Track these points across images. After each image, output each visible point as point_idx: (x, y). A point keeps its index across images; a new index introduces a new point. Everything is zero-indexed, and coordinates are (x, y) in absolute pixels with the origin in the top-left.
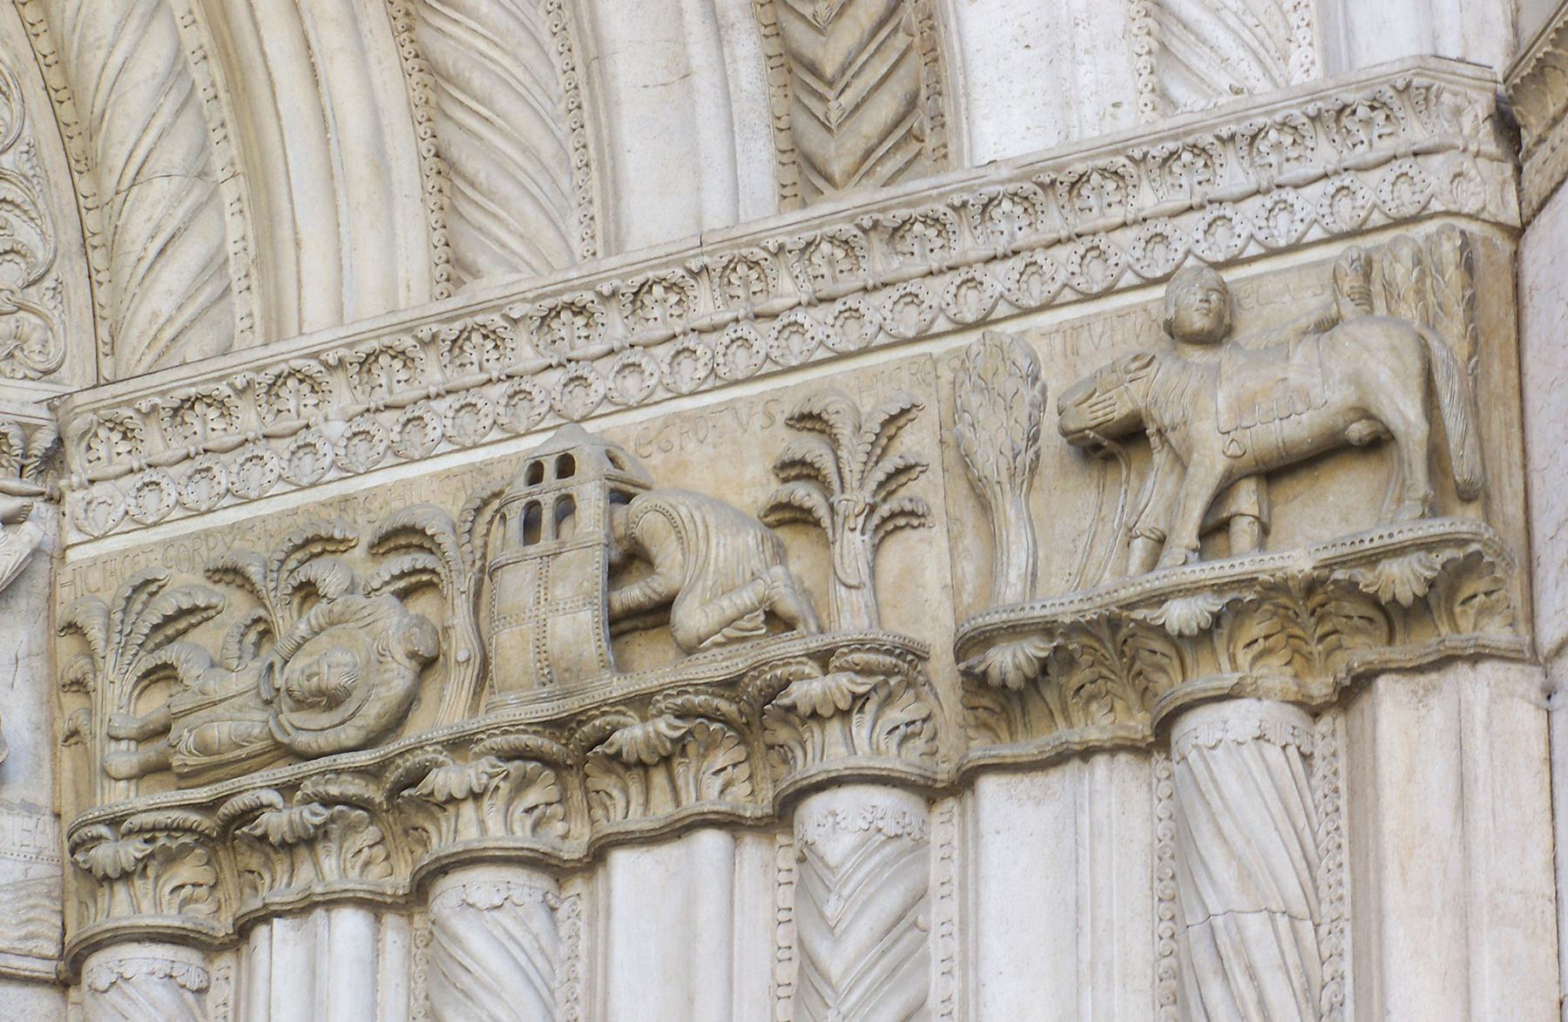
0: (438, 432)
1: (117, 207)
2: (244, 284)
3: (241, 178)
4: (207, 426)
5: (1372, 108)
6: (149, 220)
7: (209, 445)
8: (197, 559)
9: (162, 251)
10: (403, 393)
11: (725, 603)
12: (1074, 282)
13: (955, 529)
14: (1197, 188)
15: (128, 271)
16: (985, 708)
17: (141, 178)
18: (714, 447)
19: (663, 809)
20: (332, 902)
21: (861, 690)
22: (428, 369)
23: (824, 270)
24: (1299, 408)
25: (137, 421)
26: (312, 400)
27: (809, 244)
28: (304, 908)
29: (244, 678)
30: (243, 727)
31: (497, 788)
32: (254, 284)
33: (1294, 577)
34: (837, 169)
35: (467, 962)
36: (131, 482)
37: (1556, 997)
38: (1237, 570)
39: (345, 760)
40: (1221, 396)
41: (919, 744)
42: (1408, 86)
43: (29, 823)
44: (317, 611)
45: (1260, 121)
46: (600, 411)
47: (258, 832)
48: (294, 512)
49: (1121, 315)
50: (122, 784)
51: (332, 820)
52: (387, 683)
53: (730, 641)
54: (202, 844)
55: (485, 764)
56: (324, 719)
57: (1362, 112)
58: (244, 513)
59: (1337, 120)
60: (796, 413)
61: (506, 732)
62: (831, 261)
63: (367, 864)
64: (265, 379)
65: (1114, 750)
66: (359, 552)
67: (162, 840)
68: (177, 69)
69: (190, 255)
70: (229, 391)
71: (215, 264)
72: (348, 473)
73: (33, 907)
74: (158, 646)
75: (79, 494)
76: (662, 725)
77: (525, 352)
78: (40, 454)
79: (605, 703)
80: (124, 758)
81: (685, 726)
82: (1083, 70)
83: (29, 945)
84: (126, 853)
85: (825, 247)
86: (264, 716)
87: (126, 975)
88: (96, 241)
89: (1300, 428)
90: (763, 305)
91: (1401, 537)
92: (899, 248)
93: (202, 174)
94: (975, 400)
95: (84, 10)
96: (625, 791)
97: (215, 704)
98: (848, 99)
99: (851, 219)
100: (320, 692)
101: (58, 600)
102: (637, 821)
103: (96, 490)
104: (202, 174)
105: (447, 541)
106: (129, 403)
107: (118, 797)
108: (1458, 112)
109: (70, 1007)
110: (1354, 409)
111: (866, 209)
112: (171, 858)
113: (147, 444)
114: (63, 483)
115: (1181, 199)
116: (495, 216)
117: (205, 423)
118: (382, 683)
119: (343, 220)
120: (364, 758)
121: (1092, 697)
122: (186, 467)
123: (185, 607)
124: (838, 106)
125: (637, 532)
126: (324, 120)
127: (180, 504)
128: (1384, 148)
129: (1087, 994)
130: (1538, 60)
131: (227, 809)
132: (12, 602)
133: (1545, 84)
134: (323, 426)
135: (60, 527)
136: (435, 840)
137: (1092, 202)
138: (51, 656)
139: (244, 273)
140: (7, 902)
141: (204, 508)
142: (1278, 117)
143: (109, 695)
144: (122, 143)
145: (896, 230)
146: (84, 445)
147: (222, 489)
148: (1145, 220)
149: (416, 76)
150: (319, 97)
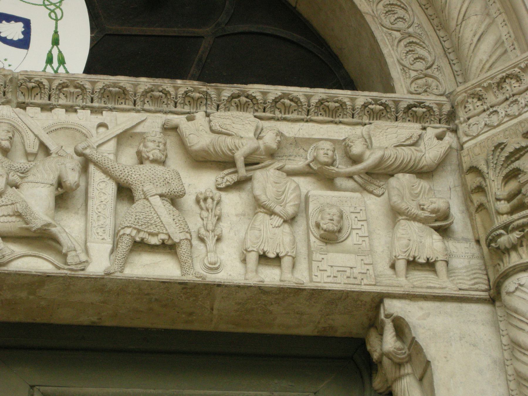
1: (457, 31)
2: (512, 47)
3: (503, 14)
4: (512, 86)
6: (472, 30)
7: (515, 92)
8: (518, 132)
9: (479, 40)
15: (467, 50)
17: (466, 18)
25: (483, 92)
32: (516, 46)
36: (484, 115)
43: (467, 245)
50: (505, 216)
69: (489, 41)
70: (519, 70)
71: (499, 42)
73: (475, 274)
74: (508, 165)
75: (464, 125)
78: (446, 113)
80: (504, 206)
83: (477, 286)
84: (513, 237)
87: (522, 283)
88: (450, 51)
93: (488, 14)
101: (463, 161)
103: (471, 121)
104: (488, 14)
106: (479, 86)
109: (497, 308)
114: (457, 122)
117: (511, 86)
122: (508, 102)
123: (517, 147)
127: (507, 115)
132: (445, 168)
135: (458, 138)
138: (464, 185)
139: (511, 44)
140: (465, 272)
141: (517, 114)
143: (493, 185)
144: (456, 8)
146: (463, 107)
147: (523, 105)
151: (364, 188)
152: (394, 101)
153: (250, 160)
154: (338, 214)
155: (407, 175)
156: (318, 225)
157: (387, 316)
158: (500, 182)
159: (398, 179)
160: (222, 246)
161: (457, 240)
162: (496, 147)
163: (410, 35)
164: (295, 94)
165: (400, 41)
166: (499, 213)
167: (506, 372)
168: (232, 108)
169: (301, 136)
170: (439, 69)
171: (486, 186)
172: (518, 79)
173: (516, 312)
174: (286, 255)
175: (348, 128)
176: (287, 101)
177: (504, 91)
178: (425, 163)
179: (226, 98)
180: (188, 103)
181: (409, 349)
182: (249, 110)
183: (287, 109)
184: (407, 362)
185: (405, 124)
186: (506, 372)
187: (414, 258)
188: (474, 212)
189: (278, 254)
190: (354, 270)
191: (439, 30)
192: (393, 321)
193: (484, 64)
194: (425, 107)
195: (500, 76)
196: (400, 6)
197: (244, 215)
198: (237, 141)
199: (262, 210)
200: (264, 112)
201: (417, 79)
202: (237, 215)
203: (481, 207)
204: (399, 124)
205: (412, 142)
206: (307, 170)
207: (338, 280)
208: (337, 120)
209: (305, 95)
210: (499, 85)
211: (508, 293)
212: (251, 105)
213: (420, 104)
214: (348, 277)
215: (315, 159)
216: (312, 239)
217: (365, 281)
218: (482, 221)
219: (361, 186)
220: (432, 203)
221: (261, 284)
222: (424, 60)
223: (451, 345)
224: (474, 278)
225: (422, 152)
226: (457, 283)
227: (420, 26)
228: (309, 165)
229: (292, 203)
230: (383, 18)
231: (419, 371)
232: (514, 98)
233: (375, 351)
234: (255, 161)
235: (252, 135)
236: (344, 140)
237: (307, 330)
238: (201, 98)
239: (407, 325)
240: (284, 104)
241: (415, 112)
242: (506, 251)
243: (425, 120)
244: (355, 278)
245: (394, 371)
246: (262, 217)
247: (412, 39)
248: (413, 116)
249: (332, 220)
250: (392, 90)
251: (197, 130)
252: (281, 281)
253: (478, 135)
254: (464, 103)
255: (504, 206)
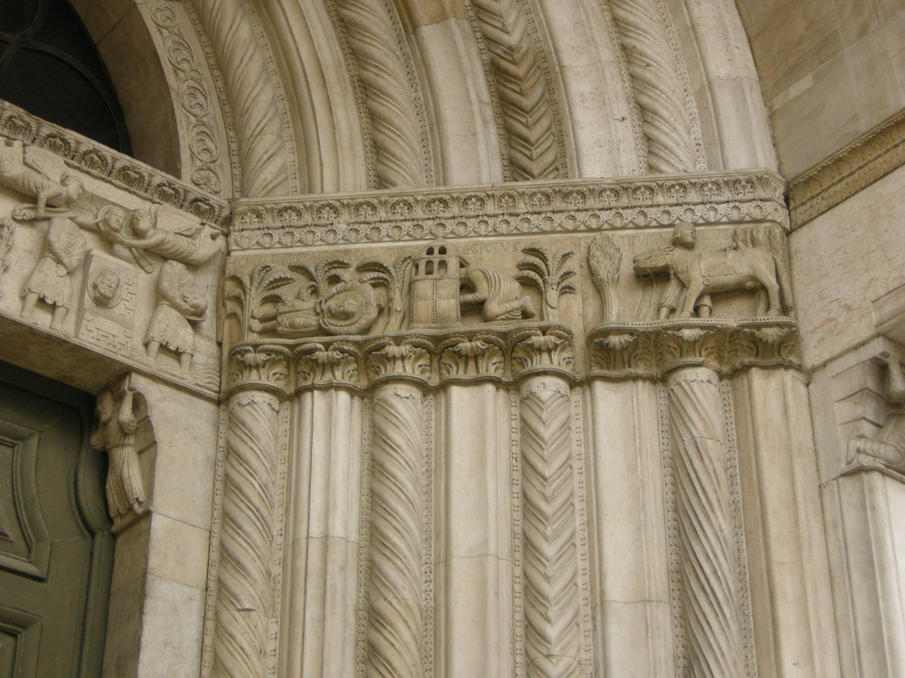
0: (385, 233)
2: (294, 176)
5: (747, 182)
7: (292, 224)
9: (269, 159)
10: (370, 218)
11: (507, 305)
12: (635, 221)
13: (585, 296)
14: (679, 198)
15: (255, 163)
16: (600, 357)
18: (494, 254)
19: (471, 374)
20: (339, 387)
21: (558, 342)
22: (381, 212)
23: (537, 203)
24: (731, 273)
26: (334, 216)
27: (534, 193)
28: (326, 388)
29: (310, 303)
30: (309, 321)
31: (411, 356)
32: (297, 176)
33: (730, 328)
34: (536, 172)
35: (396, 414)
36: (258, 232)
37: (818, 484)
38: (710, 322)
39: (351, 337)
40: (702, 265)
41: (571, 366)
42: (762, 177)
43: (209, 344)
44: (340, 286)
45: (707, 180)
46: (449, 236)
47: (314, 358)
48: (326, 252)
49: (651, 235)
50: (255, 334)
51: (343, 358)
52: (370, 314)
53: (508, 319)
54: (285, 360)
55: (408, 347)
56: (342, 323)
57: (743, 183)
58: (304, 249)
59: (734, 185)
60: (528, 248)
61: (418, 337)
62: (540, 201)
63: (351, 376)
64: (317, 205)
65: (644, 379)
66: (352, 269)
67: (273, 356)
68: (273, 102)
69: (277, 163)
71: (284, 168)
72: (347, 241)
73: (210, 373)
74: (270, 289)
76: (478, 343)
77: (419, 213)
79: (458, 332)
80: (257, 325)
81: (487, 346)
82: (623, 157)
83: (210, 386)
84: (260, 358)
85: (539, 196)
86: (317, 318)
88: (234, 153)
89: (730, 279)
90: (512, 210)
91: (770, 321)
92: (566, 200)
94: (598, 254)
95: (244, 73)
96: (457, 365)
97: (297, 311)
98: (539, 150)
99: (551, 187)
100: (344, 312)
102: (461, 375)
103: (244, 233)
104: (281, 137)
105: (392, 270)
106: (262, 205)
107: (253, 338)
108: (776, 189)
110: (751, 277)
111: (557, 185)
112: (274, 363)
113: (266, 220)
114: (231, 228)
115: (673, 201)
116: (401, 167)
117: (290, 217)
118: (368, 313)
119: (340, 159)
120: (358, 338)
121: (640, 359)
124: (535, 152)
125: (471, 277)
126: (333, 126)
127: (280, 242)
128: (750, 196)
129: (639, 458)
130: (810, 176)
131: (303, 347)
133: (809, 185)
134: (337, 225)
136: (383, 371)
137: (640, 196)
141: (289, 245)
142: (713, 179)
143: (252, 301)
145: (566, 194)
147: (297, 240)
148: (659, 206)
149: (364, 119)
150: (332, 118)
151: (137, 261)
152: (185, 190)
153: (50, 203)
154: (117, 283)
155: (180, 265)
156: (95, 287)
157: (130, 389)
158: (259, 301)
159: (173, 266)
160: (7, 277)
161: (201, 335)
162: (263, 268)
163: (204, 125)
164: (105, 153)
165: (194, 127)
166: (250, 329)
167: (215, 471)
168: (45, 145)
169: (98, 194)
170: (221, 166)
171: (245, 300)
172: (299, 214)
173: (243, 424)
174: (62, 306)
175: (139, 200)
176: (96, 158)
177: (283, 219)
178: (196, 257)
179: (44, 135)
180: (8, 127)
181: (138, 423)
182: (60, 152)
183: (92, 164)
184: (132, 434)
185: (185, 214)
186: (215, 471)
187: (167, 343)
188: (223, 316)
189: (55, 303)
190: (116, 339)
191: (230, 129)
192: (134, 395)
193: (268, 184)
194: (208, 204)
195: (284, 205)
196: (201, 92)
197: (31, 253)
198: (45, 182)
199: (52, 256)
200: (72, 159)
201: (201, 169)
202: (25, 251)
203: (234, 315)
204: (181, 211)
205: (190, 234)
206: (95, 227)
207: (101, 343)
208: (133, 189)
209: (113, 157)
210: (281, 212)
211: (239, 404)
212: (63, 149)
213: (205, 200)
214: (109, 344)
215: (106, 222)
216: (87, 297)
217: (122, 352)
218: (230, 328)
219: (135, 258)
220: (195, 298)
221: (34, 326)
222: (210, 152)
223: (177, 433)
224: (209, 377)
225: (196, 246)
226: (195, 378)
227: (214, 118)
228: (97, 224)
229: (77, 257)
230: (185, 99)
231: (142, 446)
232: (291, 230)
233: (106, 413)
234: (54, 205)
235: (58, 179)
236: (134, 211)
237: (50, 373)
238: (23, 127)
239: (145, 402)
240: (92, 159)
241: (199, 206)
242: (249, 367)
243: (204, 216)
244: (114, 346)
245: (119, 437)
246: (49, 262)
247: (205, 129)
248: (195, 209)
249: (110, 287)
250: (177, 174)
251: (13, 158)
252: (51, 328)
253: (248, 249)
254: (243, 215)
255: (257, 325)
